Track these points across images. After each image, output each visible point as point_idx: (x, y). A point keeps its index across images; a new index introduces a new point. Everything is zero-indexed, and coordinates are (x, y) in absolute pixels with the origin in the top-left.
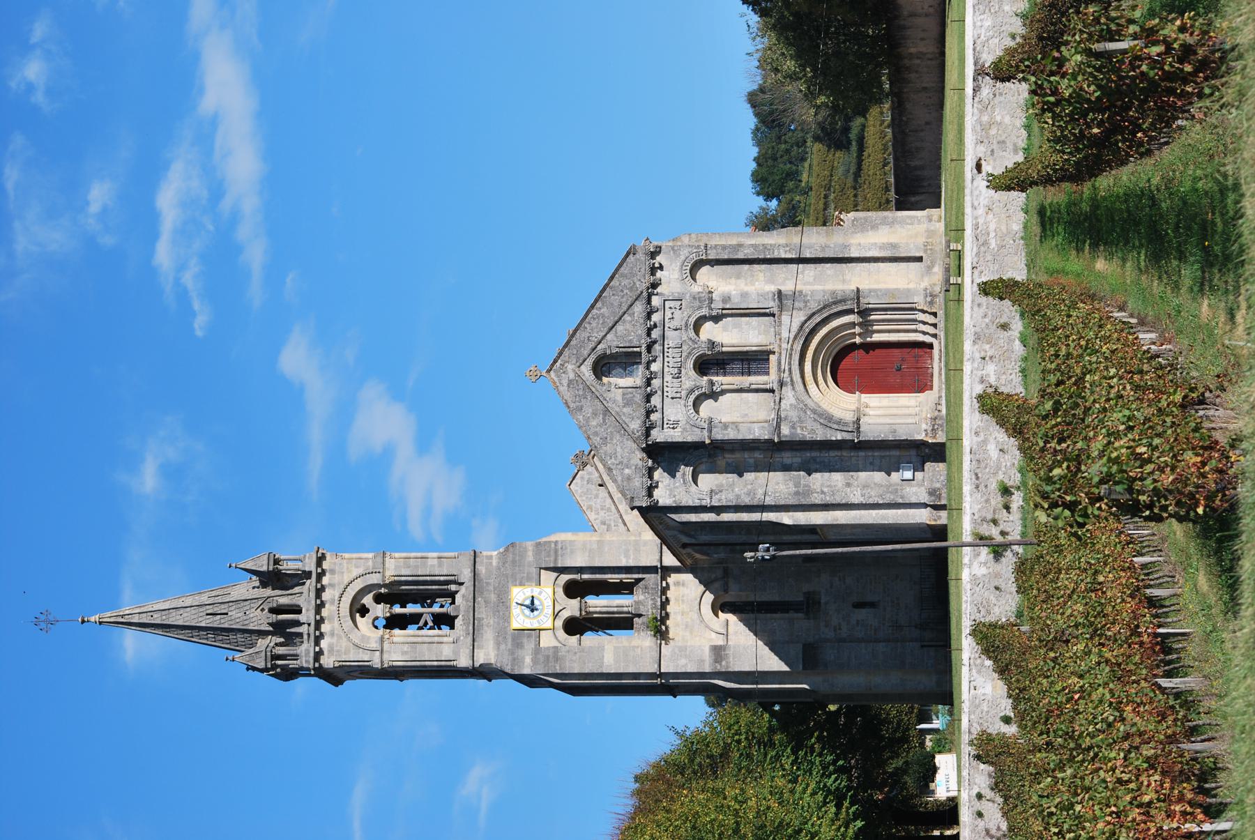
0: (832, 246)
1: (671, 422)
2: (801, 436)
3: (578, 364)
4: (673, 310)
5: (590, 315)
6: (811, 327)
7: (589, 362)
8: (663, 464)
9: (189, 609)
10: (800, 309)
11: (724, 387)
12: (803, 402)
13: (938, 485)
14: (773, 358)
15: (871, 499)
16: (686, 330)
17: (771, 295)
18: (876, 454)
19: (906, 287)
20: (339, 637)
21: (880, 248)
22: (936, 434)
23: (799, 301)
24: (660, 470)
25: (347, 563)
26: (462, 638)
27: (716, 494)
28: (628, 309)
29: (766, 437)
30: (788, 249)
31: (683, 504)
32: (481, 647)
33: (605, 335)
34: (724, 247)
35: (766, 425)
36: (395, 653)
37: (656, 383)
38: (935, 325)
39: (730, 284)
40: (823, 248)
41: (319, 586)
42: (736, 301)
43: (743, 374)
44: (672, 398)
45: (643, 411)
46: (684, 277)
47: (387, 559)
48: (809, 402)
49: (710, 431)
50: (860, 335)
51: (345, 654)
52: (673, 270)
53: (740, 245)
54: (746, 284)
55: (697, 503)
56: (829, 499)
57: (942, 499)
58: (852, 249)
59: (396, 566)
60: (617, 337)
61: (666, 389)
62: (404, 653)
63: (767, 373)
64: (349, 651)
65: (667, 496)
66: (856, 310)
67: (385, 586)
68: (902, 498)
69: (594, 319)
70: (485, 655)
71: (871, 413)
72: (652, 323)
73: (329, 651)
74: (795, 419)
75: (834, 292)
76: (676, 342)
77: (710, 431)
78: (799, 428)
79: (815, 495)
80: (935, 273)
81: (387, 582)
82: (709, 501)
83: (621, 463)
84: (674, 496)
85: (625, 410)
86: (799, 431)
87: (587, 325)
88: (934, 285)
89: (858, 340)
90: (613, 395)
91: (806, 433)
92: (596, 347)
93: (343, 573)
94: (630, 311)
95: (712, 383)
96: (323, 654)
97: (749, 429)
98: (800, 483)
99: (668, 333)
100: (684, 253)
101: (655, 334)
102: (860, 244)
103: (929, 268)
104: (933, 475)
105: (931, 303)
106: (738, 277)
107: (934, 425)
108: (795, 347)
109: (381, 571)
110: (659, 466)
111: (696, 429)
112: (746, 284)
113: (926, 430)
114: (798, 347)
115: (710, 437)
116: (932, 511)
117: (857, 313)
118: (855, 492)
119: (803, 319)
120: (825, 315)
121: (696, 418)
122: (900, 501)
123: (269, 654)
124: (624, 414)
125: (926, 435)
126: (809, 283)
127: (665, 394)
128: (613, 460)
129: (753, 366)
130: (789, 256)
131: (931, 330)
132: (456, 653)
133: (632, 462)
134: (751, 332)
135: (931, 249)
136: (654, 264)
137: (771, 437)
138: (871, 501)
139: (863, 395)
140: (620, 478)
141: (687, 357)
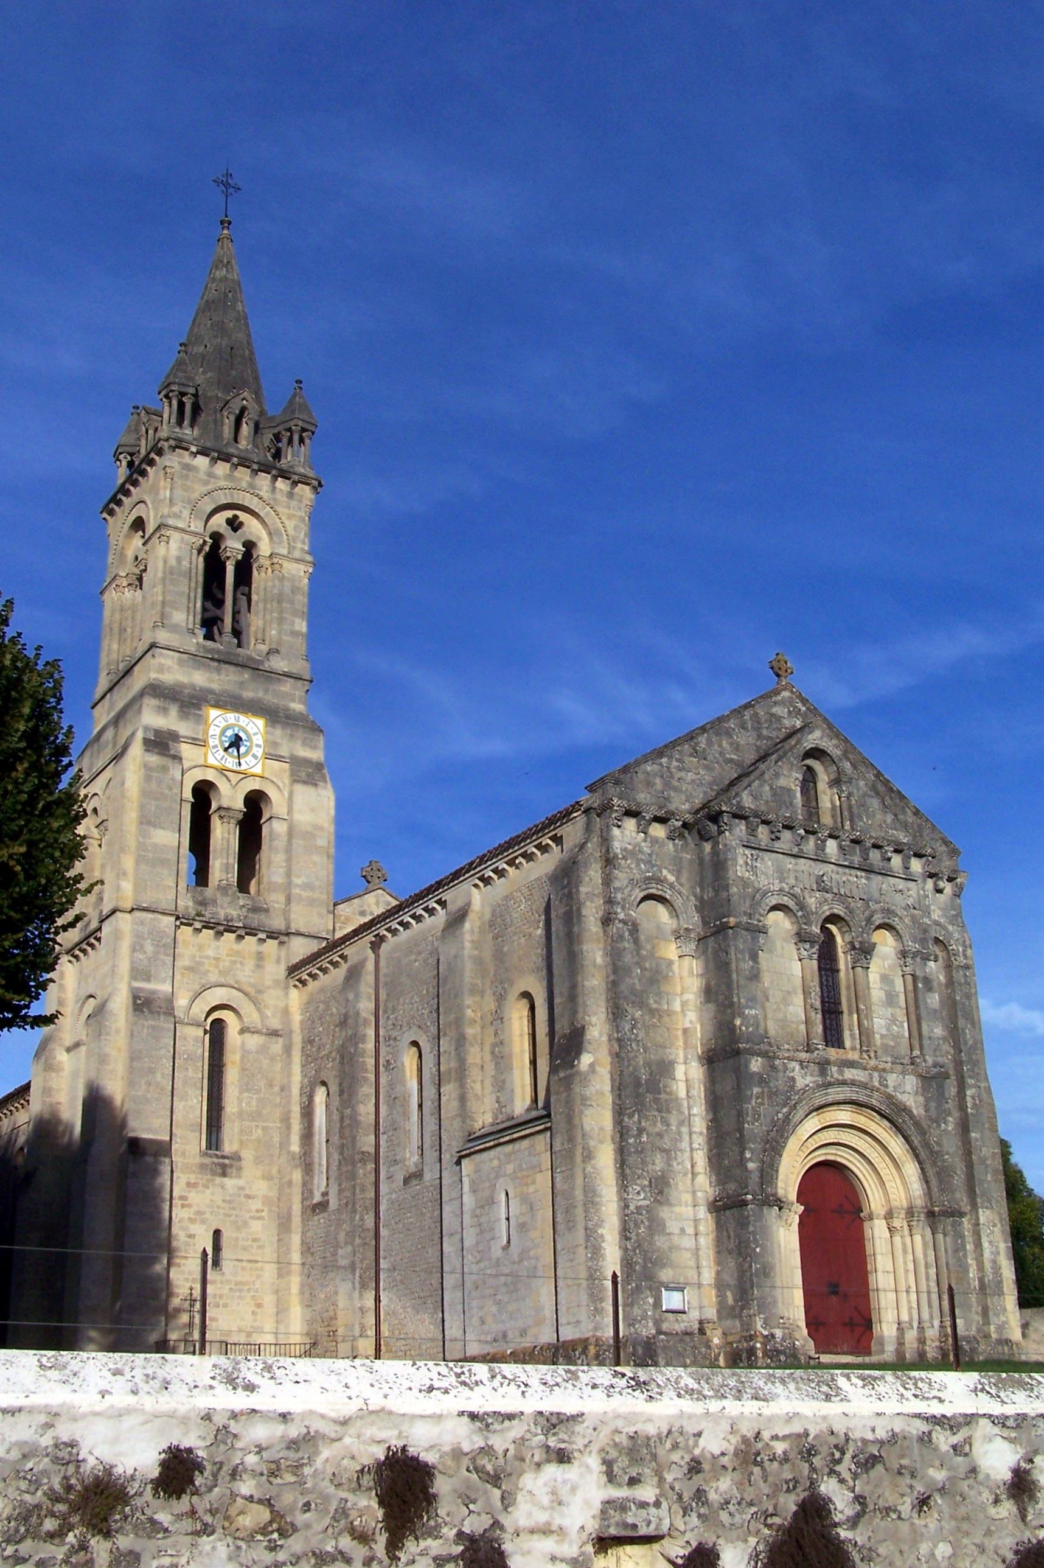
2: (749, 1093)
12: (800, 1101)
21: (994, 1262)
25: (300, 517)
32: (181, 663)
48: (801, 1113)
64: (186, 490)
70: (170, 667)
72: (889, 854)
86: (756, 1090)
90: (785, 772)
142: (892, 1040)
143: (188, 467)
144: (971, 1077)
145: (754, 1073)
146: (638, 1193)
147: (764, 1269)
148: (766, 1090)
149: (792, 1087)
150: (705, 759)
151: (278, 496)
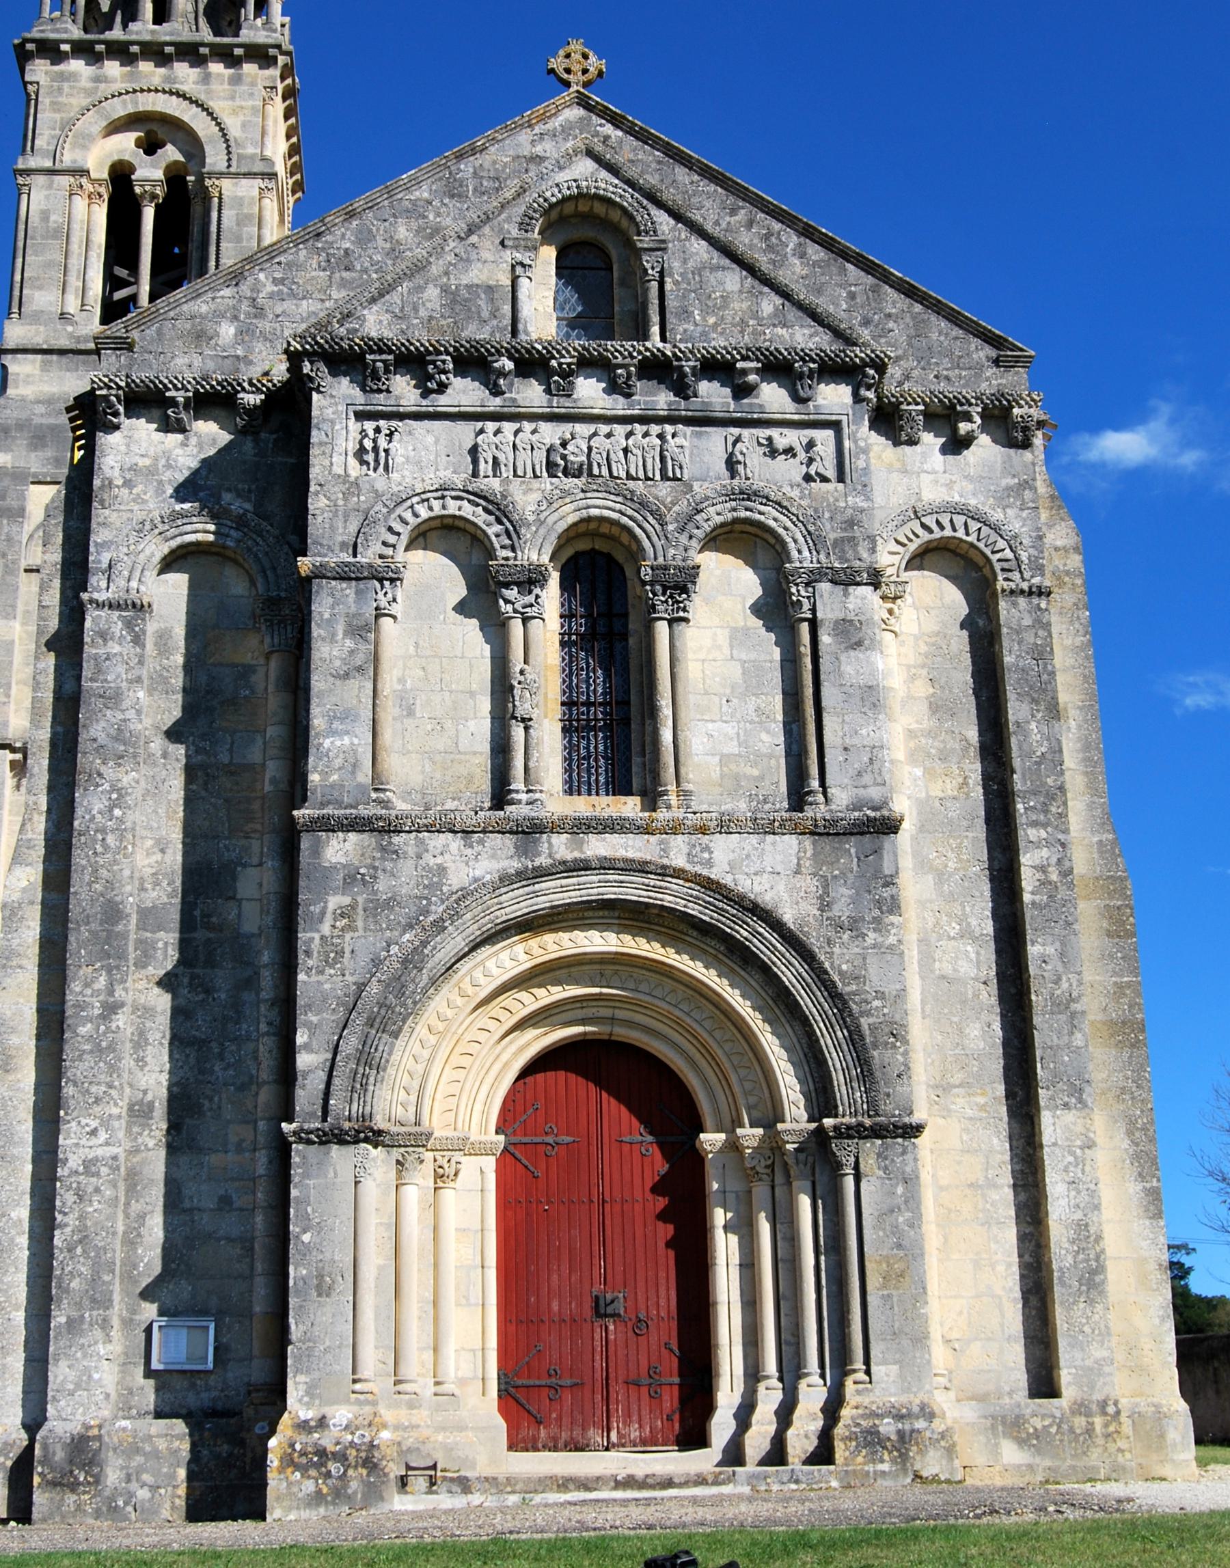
0: (1078, 1039)
1: (382, 443)
2: (314, 909)
3: (599, 148)
4: (802, 455)
5: (777, 226)
6: (757, 946)
7: (606, 184)
8: (248, 445)
10: (825, 905)
11: (516, 627)
12: (455, 915)
13: (113, 1476)
14: (630, 806)
15: (70, 1198)
16: (731, 495)
17: (875, 793)
18: (259, 1219)
19: (936, 1332)
20: (88, 92)
21: (1082, 1226)
22: (303, 1469)
23: (855, 901)
24: (225, 437)
25: (253, 107)
26: (70, 329)
27: (129, 625)
28: (800, 306)
29: (314, 778)
30: (1054, 877)
31: (99, 514)
32: (45, 367)
33: (702, 233)
34: (1042, 654)
35: (364, 776)
36: (47, 197)
37: (531, 394)
38: (777, 1455)
39: (913, 678)
40: (1064, 1005)
41: (204, 51)
42: (848, 669)
43: (568, 704)
44: (474, 451)
45: (421, 337)
46: (930, 521)
47: (258, 183)
48: (454, 942)
49: (345, 575)
50: (733, 1146)
51: (53, 103)
52: (950, 485)
53: (1054, 712)
54: (911, 734)
55: (99, 558)
56: (82, 1031)
57: (55, 1494)
58: (1069, 1117)
59: (241, 198)
60: (698, 271)
61: (509, 427)
62: (45, 216)
63: (571, 789)
64: (59, 111)
65: (129, 461)
66: (828, 1122)
67: (200, 179)
68: (73, 1325)
69: (767, 237)
71: (413, 1195)
72: (752, 378)
73: (62, 73)
74: (383, 885)
75: (897, 1034)
76: (685, 460)
77: (345, 575)
78: (347, 900)
79: (101, 983)
80: (995, 1450)
81: (208, 182)
82: (101, 597)
83: (260, 312)
85: (432, 292)
86: (335, 901)
87: (742, 215)
88: (950, 1451)
89: (711, 1140)
90: (486, 255)
91: (326, 929)
92: (660, 205)
93: (233, 98)
94: (792, 314)
95: (531, 580)
96: (52, 64)
97: (346, 716)
98: (160, 928)
99: (716, 441)
100: (1014, 521)
101: (713, 394)
102: (1090, 1145)
103: (1013, 1426)
104: (156, 1454)
105: (871, 1440)
106: (935, 707)
107: (341, 1457)
108: (675, 885)
109: (232, 170)
110: (241, 433)
111: (353, 528)
112: (911, 734)
113: (322, 1423)
114: (674, 896)
115: (319, 573)
116: (14, 1454)
117: (820, 1130)
118: (103, 1136)
119: (788, 916)
120: (804, 1001)
121: (397, 527)
122: (59, 1319)
124: (420, 289)
125: (303, 1426)
126: (927, 959)
127: (491, 426)
128: (270, 288)
129: (598, 743)
130: (1028, 880)
131: (758, 1440)
132: (37, 317)
133: (259, 346)
134: (731, 729)
135: (1090, 1431)
136: (968, 418)
137: (315, 796)
138: (65, 1198)
139: (490, 1163)
140: (204, 309)
141: (630, 497)
142: (754, 765)
143: (62, 77)
144: (1035, 824)
145: (334, 867)
146: (94, 1133)
147: (320, 1277)
148: (360, 899)
149: (434, 887)
150: (347, 269)
151: (215, 86)
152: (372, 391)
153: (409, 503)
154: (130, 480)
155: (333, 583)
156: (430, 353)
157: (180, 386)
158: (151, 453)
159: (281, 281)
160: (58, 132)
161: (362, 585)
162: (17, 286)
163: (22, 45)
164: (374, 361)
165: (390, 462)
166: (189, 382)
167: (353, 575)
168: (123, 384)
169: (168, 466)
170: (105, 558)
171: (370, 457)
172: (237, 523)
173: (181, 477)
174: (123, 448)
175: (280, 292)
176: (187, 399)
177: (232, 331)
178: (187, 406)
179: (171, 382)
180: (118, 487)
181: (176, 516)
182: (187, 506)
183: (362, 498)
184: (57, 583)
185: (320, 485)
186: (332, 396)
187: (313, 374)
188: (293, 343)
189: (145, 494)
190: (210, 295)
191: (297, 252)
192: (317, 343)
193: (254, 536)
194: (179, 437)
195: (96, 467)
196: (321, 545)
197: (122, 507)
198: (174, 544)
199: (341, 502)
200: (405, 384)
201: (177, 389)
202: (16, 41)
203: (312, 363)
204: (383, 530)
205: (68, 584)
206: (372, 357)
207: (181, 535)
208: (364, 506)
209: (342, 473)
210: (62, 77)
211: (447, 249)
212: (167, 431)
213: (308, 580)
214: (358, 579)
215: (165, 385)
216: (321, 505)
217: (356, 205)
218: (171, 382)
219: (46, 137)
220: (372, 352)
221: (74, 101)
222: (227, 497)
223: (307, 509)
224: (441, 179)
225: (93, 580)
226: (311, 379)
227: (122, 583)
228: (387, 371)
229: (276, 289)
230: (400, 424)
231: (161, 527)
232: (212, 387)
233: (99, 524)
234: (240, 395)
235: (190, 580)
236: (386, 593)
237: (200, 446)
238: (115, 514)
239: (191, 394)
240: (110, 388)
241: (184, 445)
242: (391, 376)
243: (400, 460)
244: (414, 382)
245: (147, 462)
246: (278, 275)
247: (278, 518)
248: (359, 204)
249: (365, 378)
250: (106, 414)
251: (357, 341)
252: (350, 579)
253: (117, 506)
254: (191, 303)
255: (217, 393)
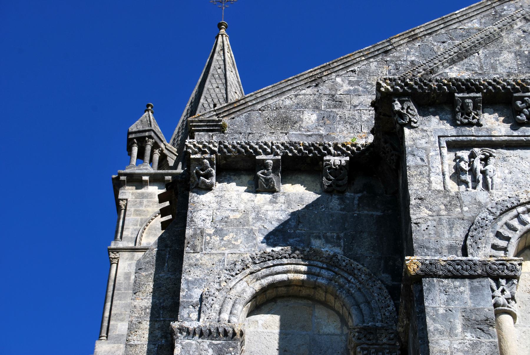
1: (478, 165)
8: (335, 202)
9: (224, 91)
24: (311, 197)
51: (136, 211)
64: (140, 215)
65: (220, 215)
82: (192, 325)
84: (218, 232)
96: (137, 189)
110: (327, 192)
111: (459, 234)
121: (506, 232)
123: (147, 134)
124: (495, 54)
128: (346, 87)
140: (288, 102)
143: (143, 196)
152: (463, 125)
153: (514, 212)
154: (222, 230)
155: (446, 281)
156: (517, 91)
157: (269, 150)
158: (242, 207)
159: (357, 83)
160: (138, 227)
161: (476, 283)
162: (106, 320)
163: (118, 178)
164: (463, 99)
165: (489, 180)
166: (278, 147)
167: (466, 273)
168: (216, 149)
169: (258, 218)
170: (196, 294)
171: (468, 178)
172: (327, 264)
173: (271, 228)
174: (215, 205)
175: (355, 90)
176: (276, 162)
177: (314, 117)
178: (275, 170)
179: (261, 147)
180: (210, 235)
181: (265, 258)
182: (278, 249)
183: (465, 209)
184: (146, 325)
185: (421, 199)
186: (423, 130)
187: (405, 112)
188: (384, 85)
189: (236, 240)
190: (293, 93)
191: (369, 64)
192: (407, 84)
193: (346, 275)
194: (268, 197)
195: (188, 220)
196: (428, 248)
197: (213, 251)
198: (265, 282)
199: (443, 213)
200: (493, 120)
201: (267, 153)
202: (114, 176)
203: (402, 103)
204: (492, 235)
205: (157, 325)
206: (461, 95)
207: (272, 274)
208: (467, 215)
209: (442, 189)
210: (143, 196)
211: (516, 27)
212: (256, 191)
213: (418, 279)
214: (471, 277)
215: (255, 150)
216: (423, 215)
217: (417, 31)
218: (261, 147)
219: (130, 230)
220: (461, 91)
221: (150, 209)
222: (316, 243)
223: (410, 219)
224: (488, 15)
225: (183, 312)
226: (401, 116)
227: (214, 315)
228: (476, 108)
229: (352, 88)
230: (494, 150)
231: (252, 268)
232: (300, 151)
233: (190, 265)
234: (326, 158)
235: (281, 320)
236: (503, 291)
237: (289, 203)
238: (207, 257)
239: (280, 157)
240: (205, 153)
241: (273, 202)
242: (480, 112)
243: (497, 181)
244: (502, 118)
245: (238, 215)
246: (351, 79)
247: (368, 259)
248: (420, 30)
249: (454, 113)
250: (199, 175)
251: (446, 82)
252: (463, 277)
253: (208, 251)
254: (275, 99)
255: (304, 157)
